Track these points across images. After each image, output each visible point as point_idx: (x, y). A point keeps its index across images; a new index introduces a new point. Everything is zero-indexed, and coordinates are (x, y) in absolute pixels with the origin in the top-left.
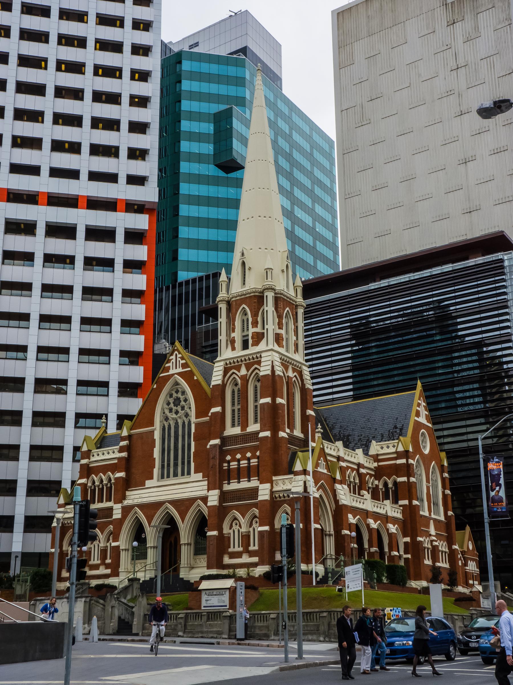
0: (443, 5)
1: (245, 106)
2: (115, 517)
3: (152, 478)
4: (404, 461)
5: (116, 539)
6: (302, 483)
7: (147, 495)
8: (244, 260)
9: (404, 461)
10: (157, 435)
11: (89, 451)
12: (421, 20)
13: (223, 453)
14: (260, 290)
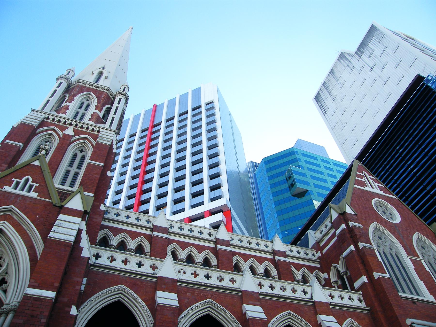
0: (352, 57)
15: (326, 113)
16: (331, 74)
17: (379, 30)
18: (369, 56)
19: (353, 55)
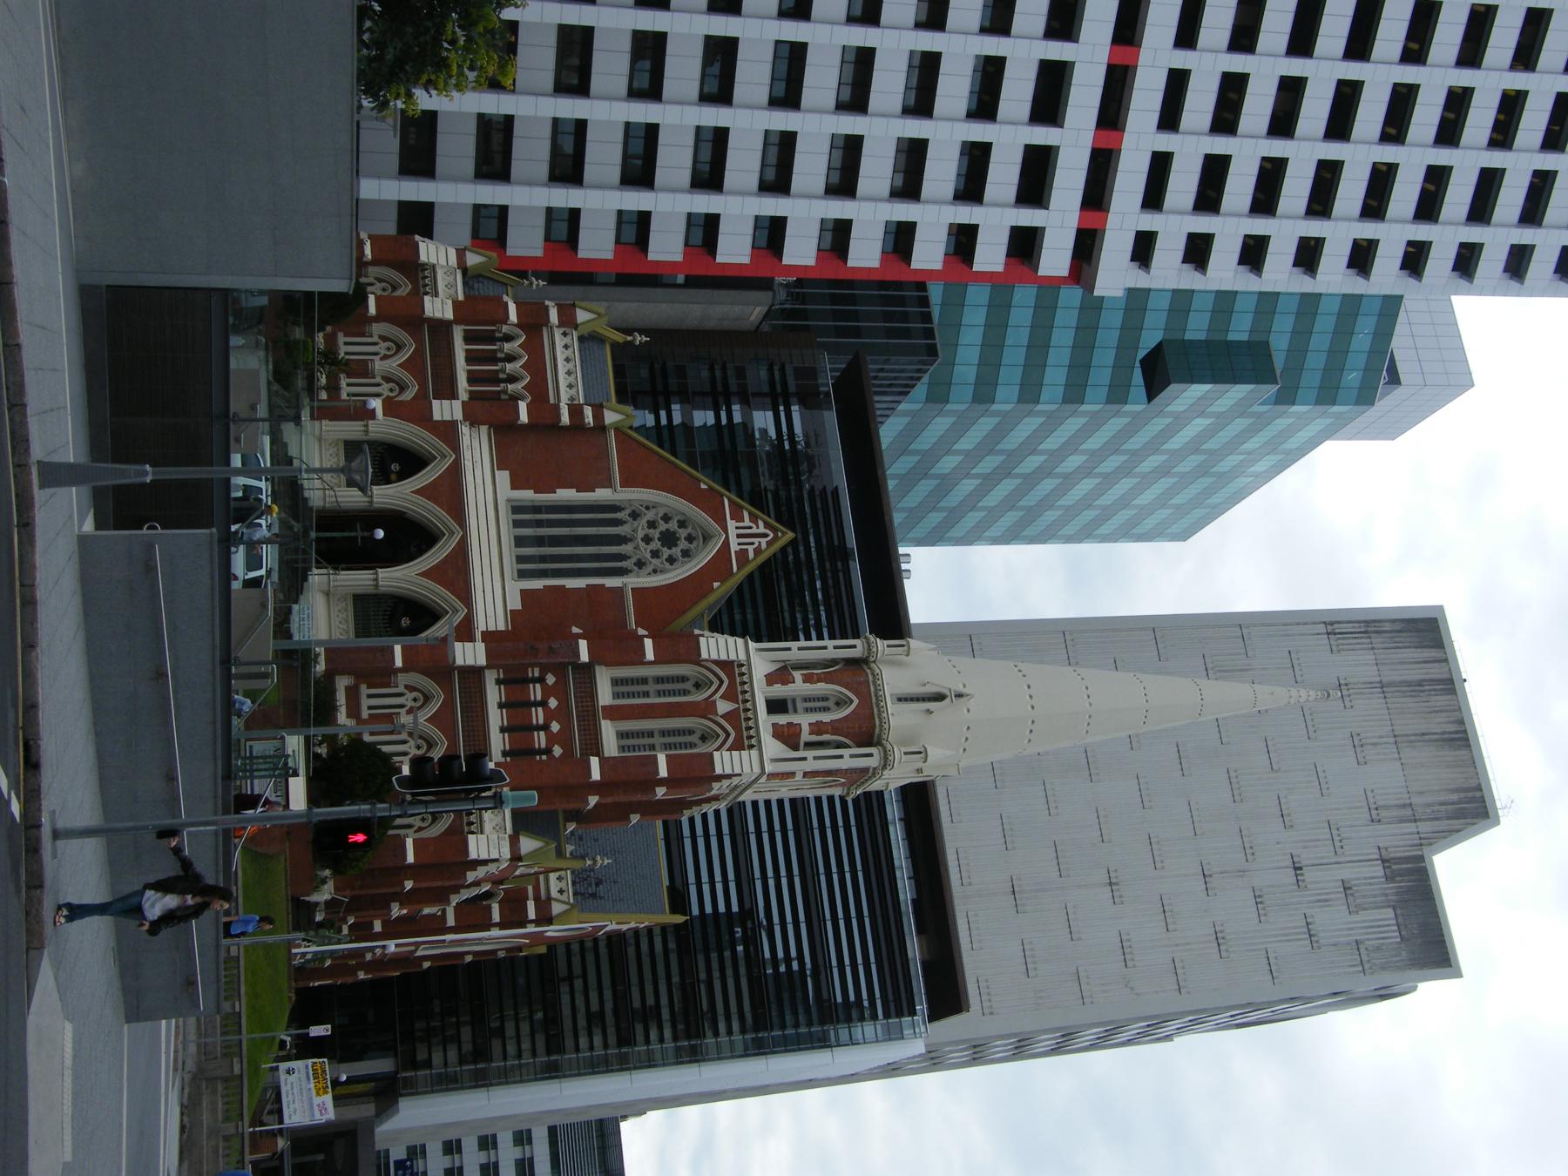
0: (1420, 838)
1: (1275, 404)
2: (436, 404)
3: (514, 487)
4: (532, 915)
5: (391, 408)
6: (494, 855)
7: (479, 481)
8: (947, 701)
9: (532, 915)
10: (602, 495)
11: (576, 327)
12: (1401, 793)
13: (559, 670)
14: (885, 737)
15: (1328, 634)
16: (1450, 733)
17: (1399, 968)
18: (1350, 888)
19: (1421, 845)
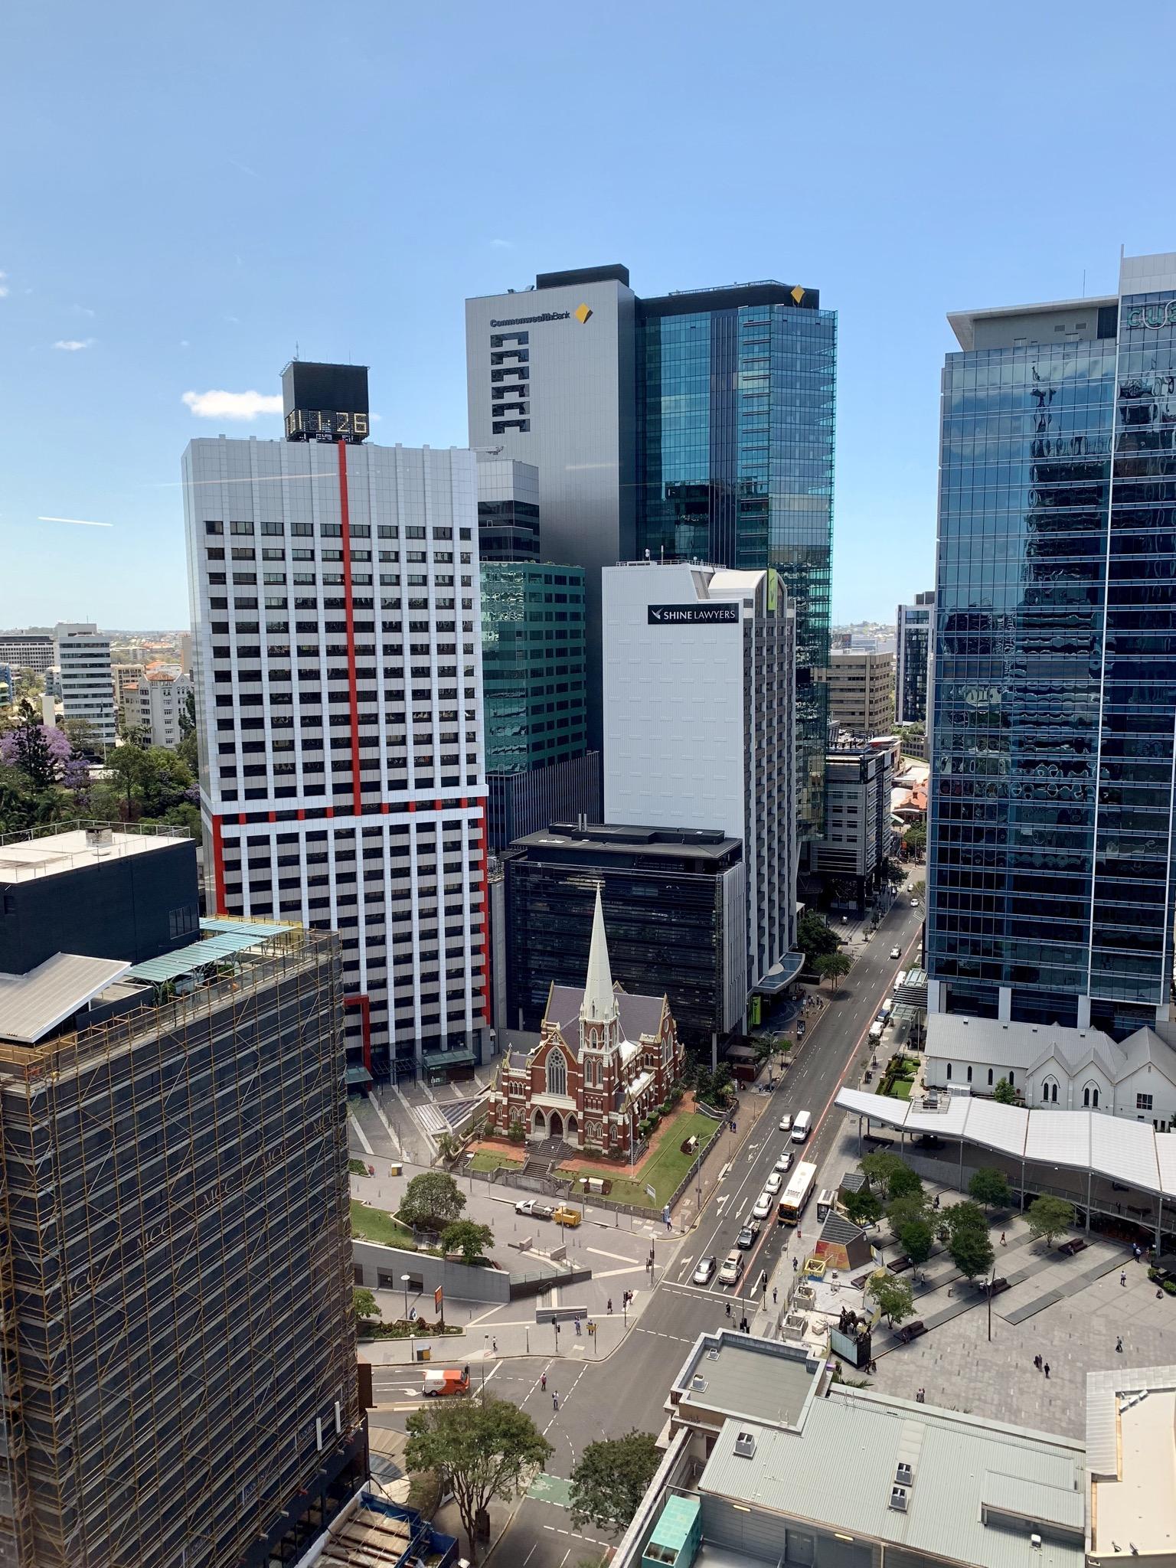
10: (547, 1072)
